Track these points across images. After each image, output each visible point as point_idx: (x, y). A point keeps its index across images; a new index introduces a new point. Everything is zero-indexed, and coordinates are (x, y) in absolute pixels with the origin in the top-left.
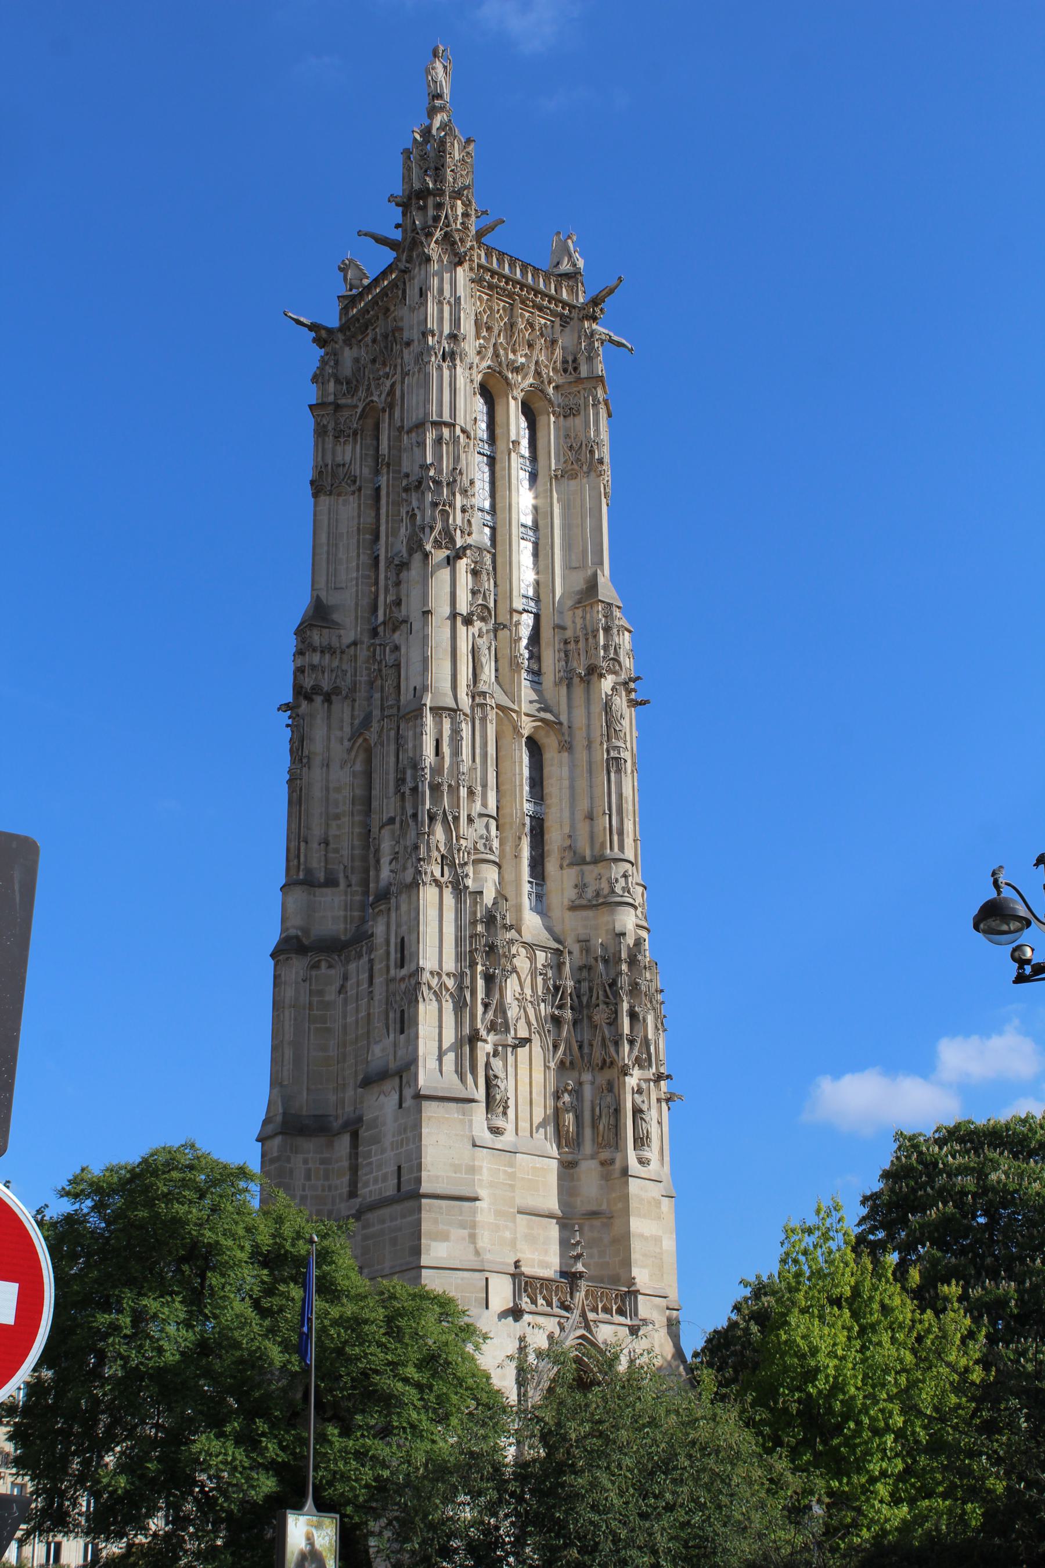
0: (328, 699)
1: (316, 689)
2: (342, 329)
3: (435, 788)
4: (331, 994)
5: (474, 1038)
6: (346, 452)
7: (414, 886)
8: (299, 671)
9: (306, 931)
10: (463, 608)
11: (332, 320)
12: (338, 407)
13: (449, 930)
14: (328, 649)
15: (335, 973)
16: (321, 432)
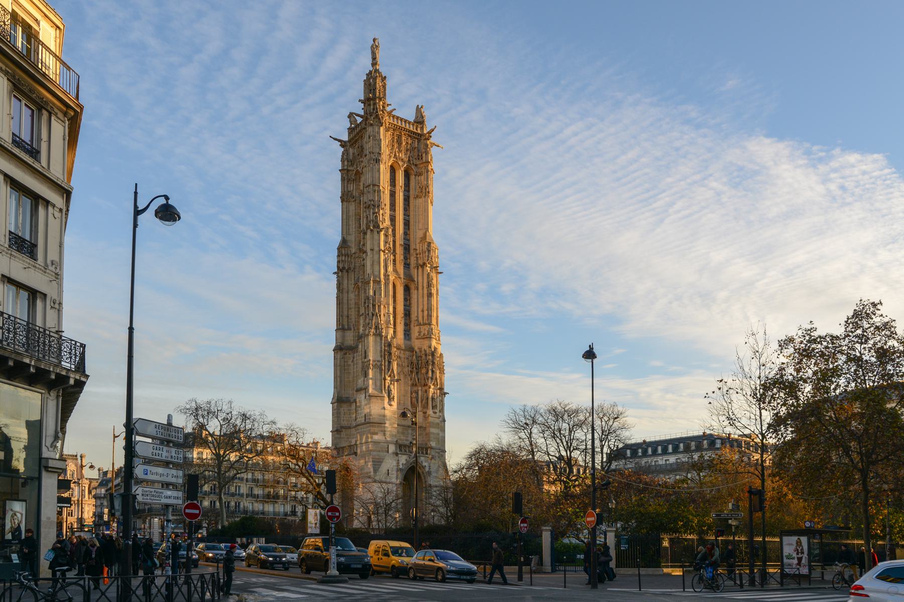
0: (347, 271)
1: (344, 268)
2: (349, 141)
3: (374, 306)
4: (350, 362)
5: (385, 379)
6: (351, 187)
7: (368, 335)
8: (338, 262)
9: (342, 343)
10: (382, 247)
11: (345, 138)
12: (348, 171)
13: (379, 348)
14: (347, 255)
15: (351, 356)
16: (343, 179)
